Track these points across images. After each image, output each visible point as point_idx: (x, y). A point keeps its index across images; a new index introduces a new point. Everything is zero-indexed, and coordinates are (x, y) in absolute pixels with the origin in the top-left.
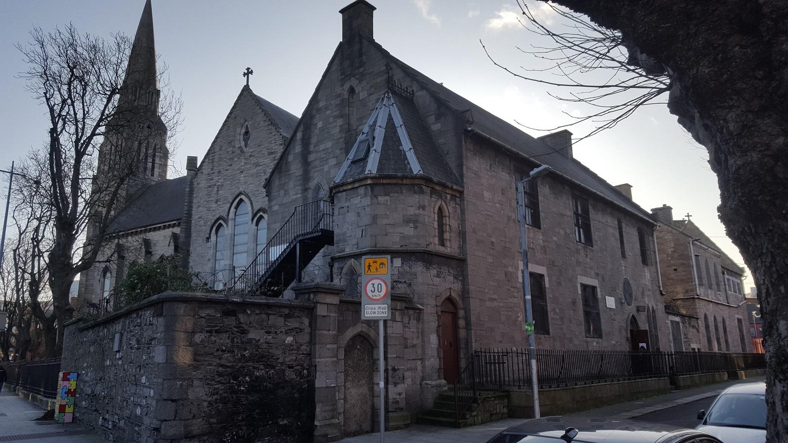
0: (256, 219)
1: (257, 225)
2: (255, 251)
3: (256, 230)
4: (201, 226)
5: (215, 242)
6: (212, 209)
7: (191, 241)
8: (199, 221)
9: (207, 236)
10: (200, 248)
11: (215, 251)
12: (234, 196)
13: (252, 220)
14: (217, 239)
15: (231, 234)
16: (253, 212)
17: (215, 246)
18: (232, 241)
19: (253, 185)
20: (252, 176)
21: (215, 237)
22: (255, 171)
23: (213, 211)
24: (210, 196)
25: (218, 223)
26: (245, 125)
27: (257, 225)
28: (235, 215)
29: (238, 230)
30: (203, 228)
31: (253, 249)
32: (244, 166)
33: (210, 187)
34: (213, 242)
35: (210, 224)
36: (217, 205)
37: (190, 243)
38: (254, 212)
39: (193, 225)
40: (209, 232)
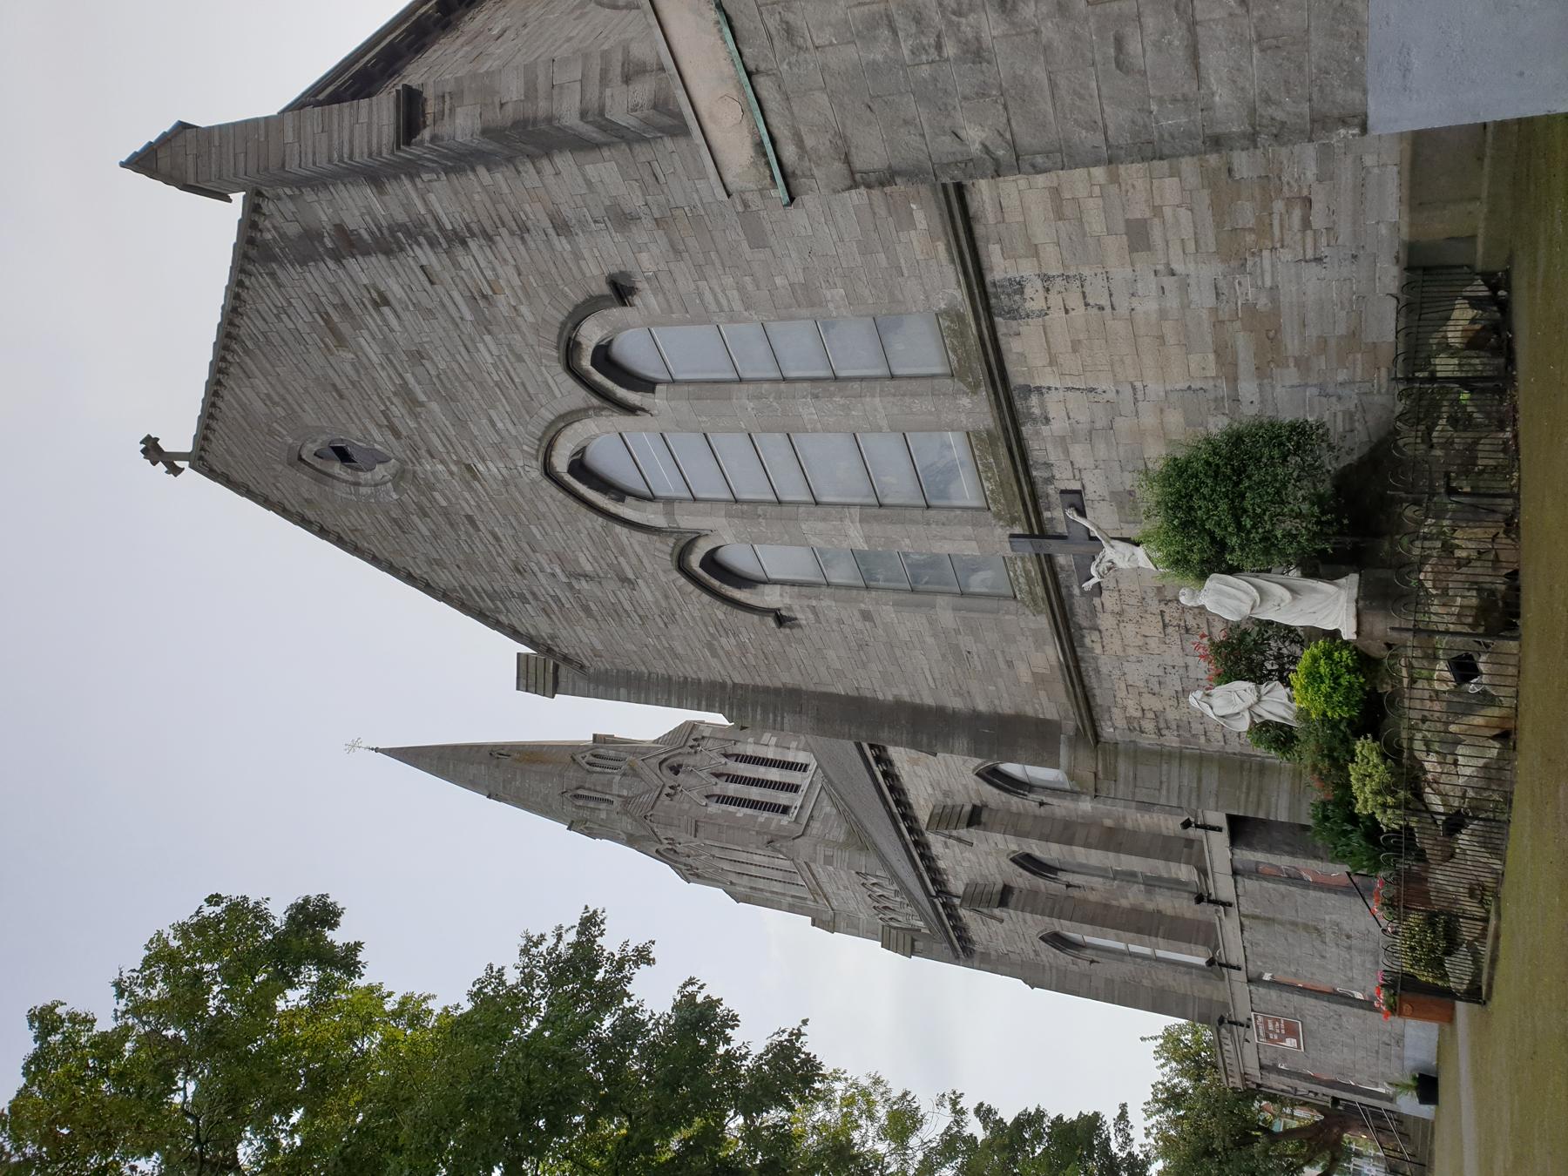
0: (621, 393)
1: (648, 385)
2: (766, 386)
3: (672, 388)
4: (742, 647)
5: (787, 588)
6: (664, 604)
7: (812, 687)
8: (727, 654)
9: (771, 622)
10: (831, 654)
11: (824, 589)
12: (583, 510)
13: (631, 410)
14: (776, 582)
15: (728, 515)
16: (598, 411)
17: (805, 590)
18: (760, 510)
19: (492, 412)
20: (460, 422)
21: (767, 589)
22: (434, 406)
23: (666, 597)
24: (621, 611)
25: (700, 571)
26: (318, 463)
27: (648, 385)
28: (652, 498)
29: (708, 485)
30: (744, 638)
31: (759, 397)
32: (442, 462)
33: (587, 609)
34: (787, 601)
35: (720, 611)
36: (640, 581)
37: (825, 694)
38: (595, 401)
39: (749, 681)
40: (756, 618)
